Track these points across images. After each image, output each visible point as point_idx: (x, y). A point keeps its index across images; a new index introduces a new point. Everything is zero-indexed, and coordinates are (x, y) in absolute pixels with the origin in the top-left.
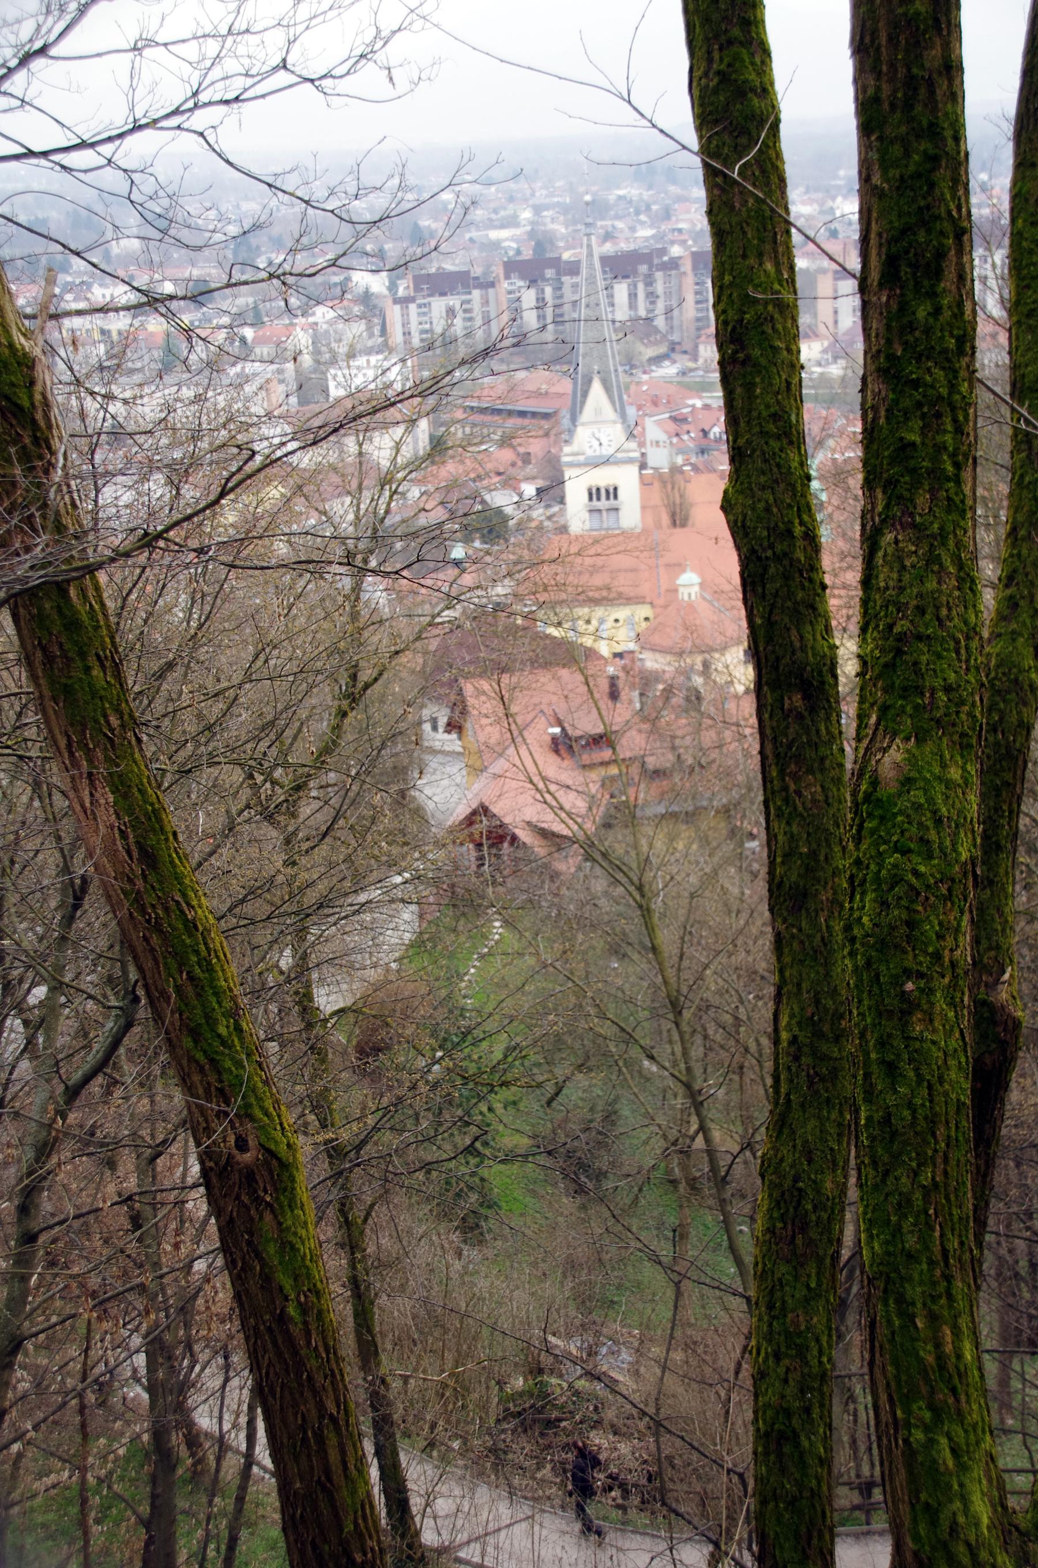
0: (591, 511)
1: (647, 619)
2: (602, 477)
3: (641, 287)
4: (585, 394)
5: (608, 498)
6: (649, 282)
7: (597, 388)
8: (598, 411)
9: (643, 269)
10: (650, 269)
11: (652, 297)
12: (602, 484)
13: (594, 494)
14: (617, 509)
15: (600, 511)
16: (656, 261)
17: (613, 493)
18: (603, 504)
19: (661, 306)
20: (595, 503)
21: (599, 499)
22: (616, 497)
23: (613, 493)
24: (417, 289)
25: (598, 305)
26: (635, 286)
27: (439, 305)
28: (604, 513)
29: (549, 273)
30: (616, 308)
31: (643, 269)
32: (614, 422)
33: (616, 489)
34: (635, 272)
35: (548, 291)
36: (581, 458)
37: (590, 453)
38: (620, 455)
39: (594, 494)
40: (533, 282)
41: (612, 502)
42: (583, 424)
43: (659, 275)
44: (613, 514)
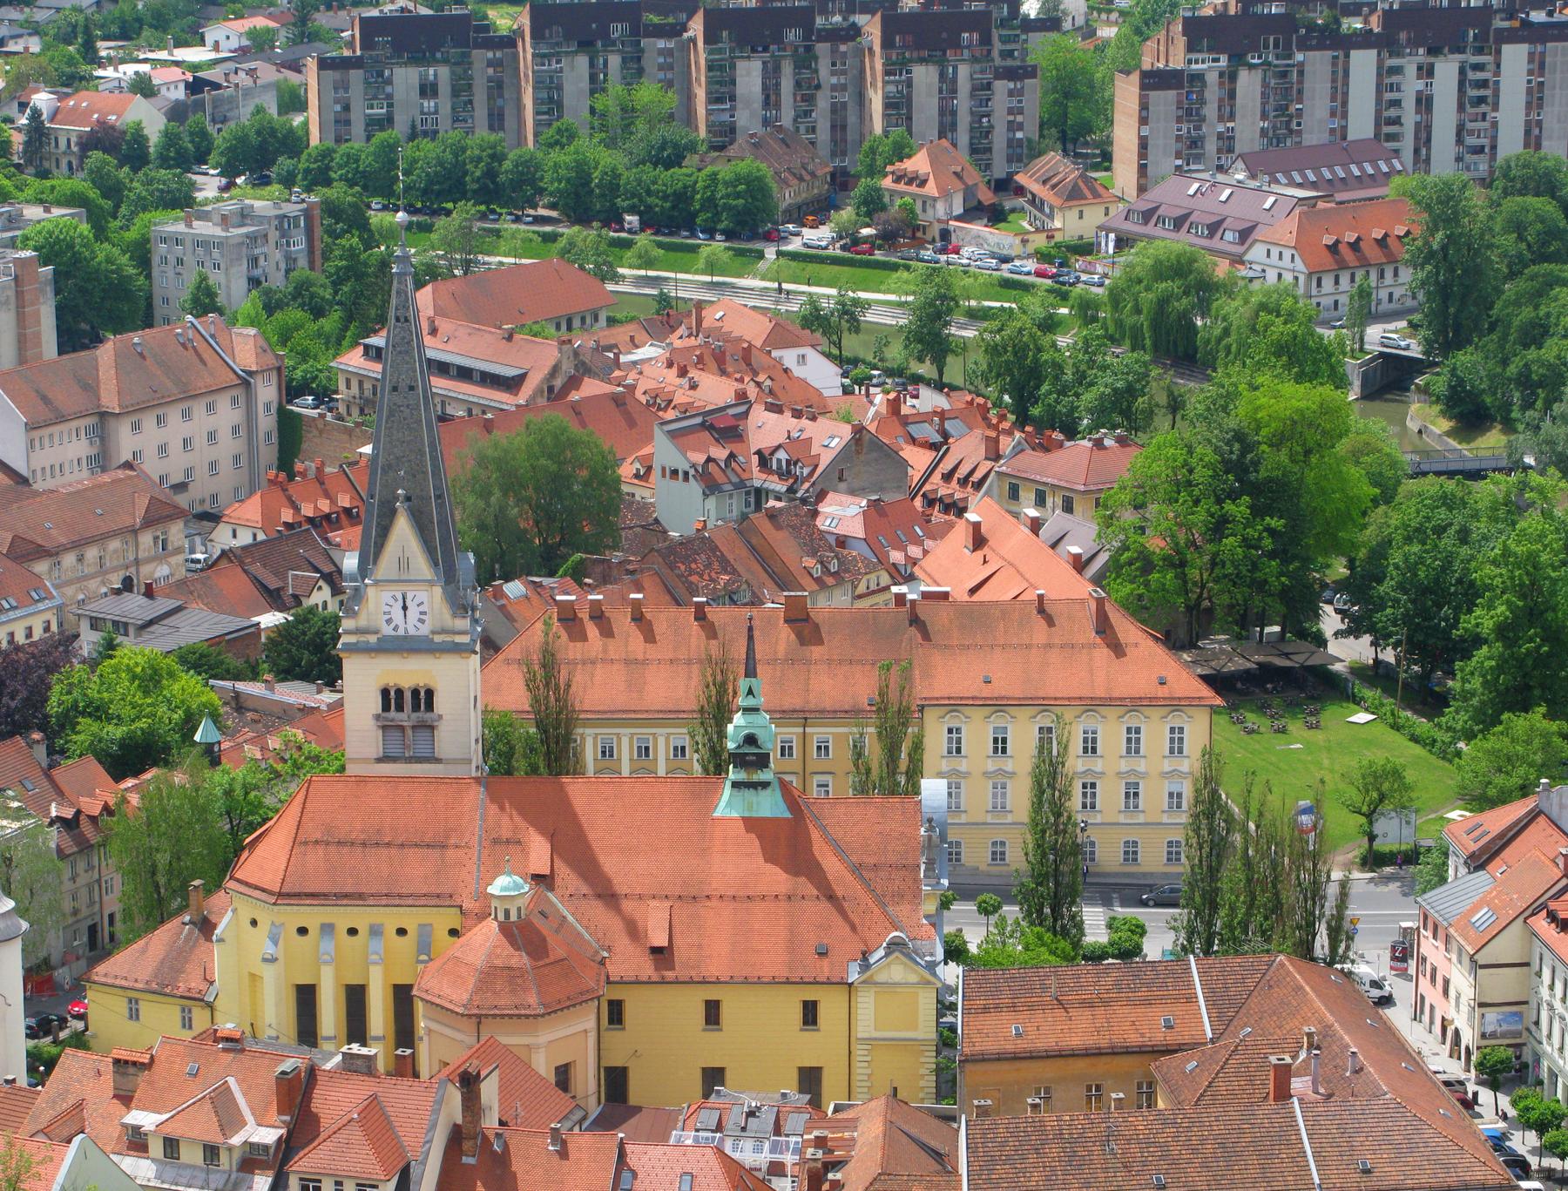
0: (384, 728)
1: (454, 932)
2: (408, 672)
3: (787, 69)
4: (384, 531)
5: (416, 708)
6: (805, 61)
7: (402, 528)
8: (403, 563)
9: (792, 35)
10: (807, 37)
11: (807, 91)
12: (407, 683)
13: (391, 698)
14: (432, 728)
15: (402, 728)
16: (819, 21)
17: (424, 699)
18: (406, 718)
19: (823, 102)
20: (393, 714)
21: (400, 708)
22: (430, 706)
23: (424, 699)
24: (367, 43)
25: (412, 388)
26: (777, 69)
27: (405, 78)
28: (409, 732)
29: (617, 30)
30: (739, 105)
31: (792, 35)
32: (431, 583)
33: (430, 693)
34: (779, 40)
35: (614, 61)
36: (373, 639)
37: (387, 630)
38: (438, 639)
39: (391, 698)
40: (586, 45)
41: (422, 715)
42: (377, 583)
43: (822, 48)
44: (425, 734)
